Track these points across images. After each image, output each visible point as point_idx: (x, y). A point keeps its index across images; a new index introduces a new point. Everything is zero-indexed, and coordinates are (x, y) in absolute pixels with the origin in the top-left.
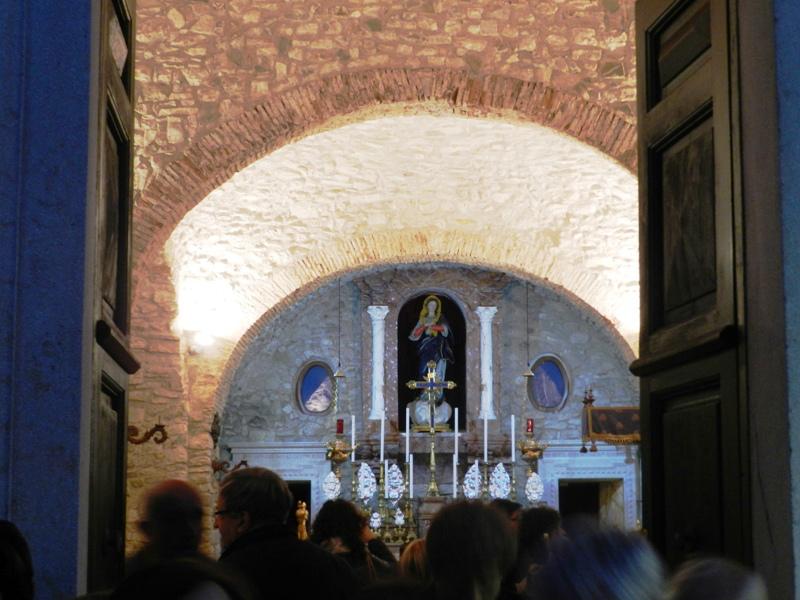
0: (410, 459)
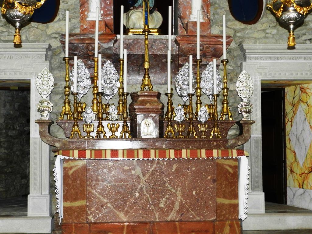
0: (123, 54)
